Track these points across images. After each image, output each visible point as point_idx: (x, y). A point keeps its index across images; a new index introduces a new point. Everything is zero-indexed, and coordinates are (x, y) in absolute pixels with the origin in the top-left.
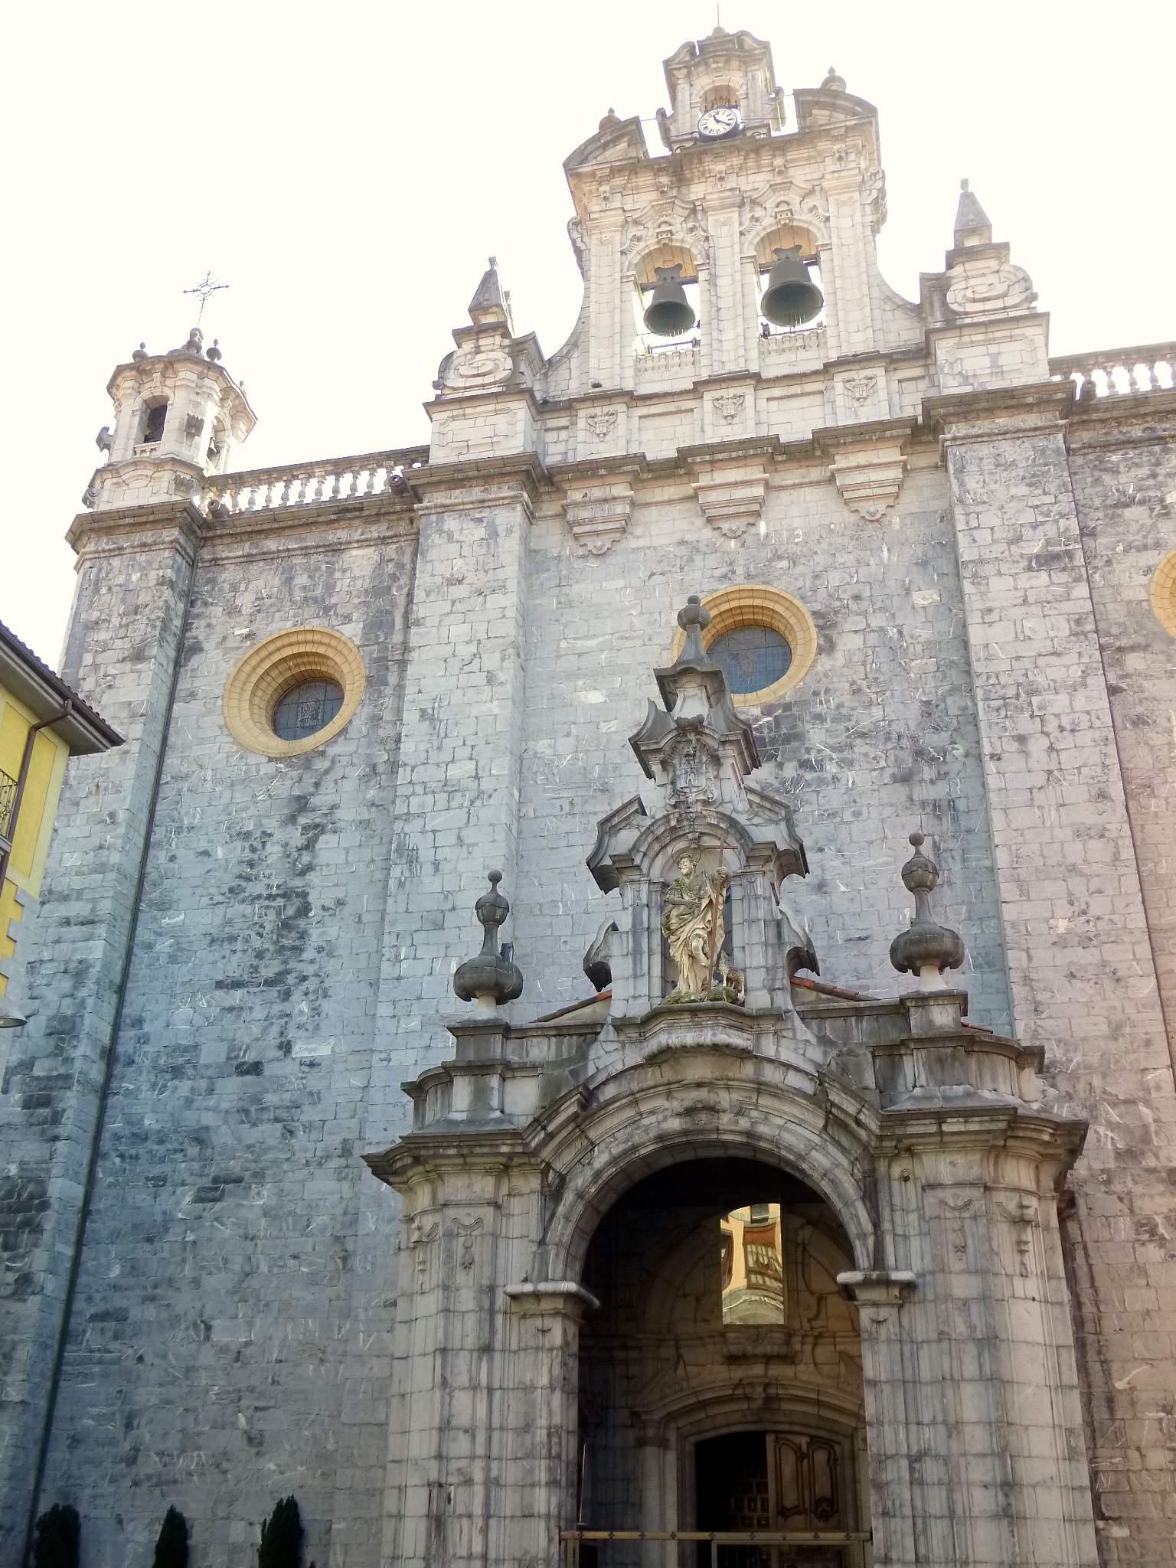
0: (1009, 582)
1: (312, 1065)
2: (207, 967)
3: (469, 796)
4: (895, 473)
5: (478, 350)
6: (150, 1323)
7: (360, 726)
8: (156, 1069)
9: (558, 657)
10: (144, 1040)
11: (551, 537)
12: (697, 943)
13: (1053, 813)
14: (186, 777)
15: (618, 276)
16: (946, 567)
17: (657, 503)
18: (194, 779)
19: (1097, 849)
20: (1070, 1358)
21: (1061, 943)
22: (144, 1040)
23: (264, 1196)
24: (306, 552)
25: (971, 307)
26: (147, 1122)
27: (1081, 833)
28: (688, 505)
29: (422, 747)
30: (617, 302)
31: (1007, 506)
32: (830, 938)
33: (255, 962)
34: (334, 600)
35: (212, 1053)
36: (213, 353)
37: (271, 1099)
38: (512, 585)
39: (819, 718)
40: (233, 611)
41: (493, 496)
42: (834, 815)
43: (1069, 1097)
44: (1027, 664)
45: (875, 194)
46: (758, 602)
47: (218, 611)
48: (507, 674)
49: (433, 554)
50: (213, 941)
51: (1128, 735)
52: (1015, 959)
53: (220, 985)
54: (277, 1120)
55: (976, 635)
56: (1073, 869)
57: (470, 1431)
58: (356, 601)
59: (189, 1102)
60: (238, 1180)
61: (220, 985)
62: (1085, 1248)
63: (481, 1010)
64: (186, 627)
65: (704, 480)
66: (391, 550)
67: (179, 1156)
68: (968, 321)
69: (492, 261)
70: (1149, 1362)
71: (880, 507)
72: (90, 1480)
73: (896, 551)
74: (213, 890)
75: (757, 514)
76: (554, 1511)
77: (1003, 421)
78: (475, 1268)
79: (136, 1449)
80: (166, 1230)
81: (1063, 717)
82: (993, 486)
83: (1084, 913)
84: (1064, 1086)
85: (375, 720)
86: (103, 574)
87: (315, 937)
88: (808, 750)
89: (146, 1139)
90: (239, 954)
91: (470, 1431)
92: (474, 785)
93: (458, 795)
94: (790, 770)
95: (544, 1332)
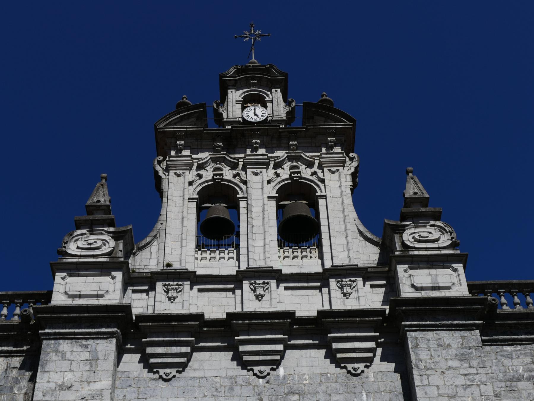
25: (417, 245)
31: (447, 372)
49: (50, 366)
71: (361, 366)
73: (372, 396)
82: (437, 359)
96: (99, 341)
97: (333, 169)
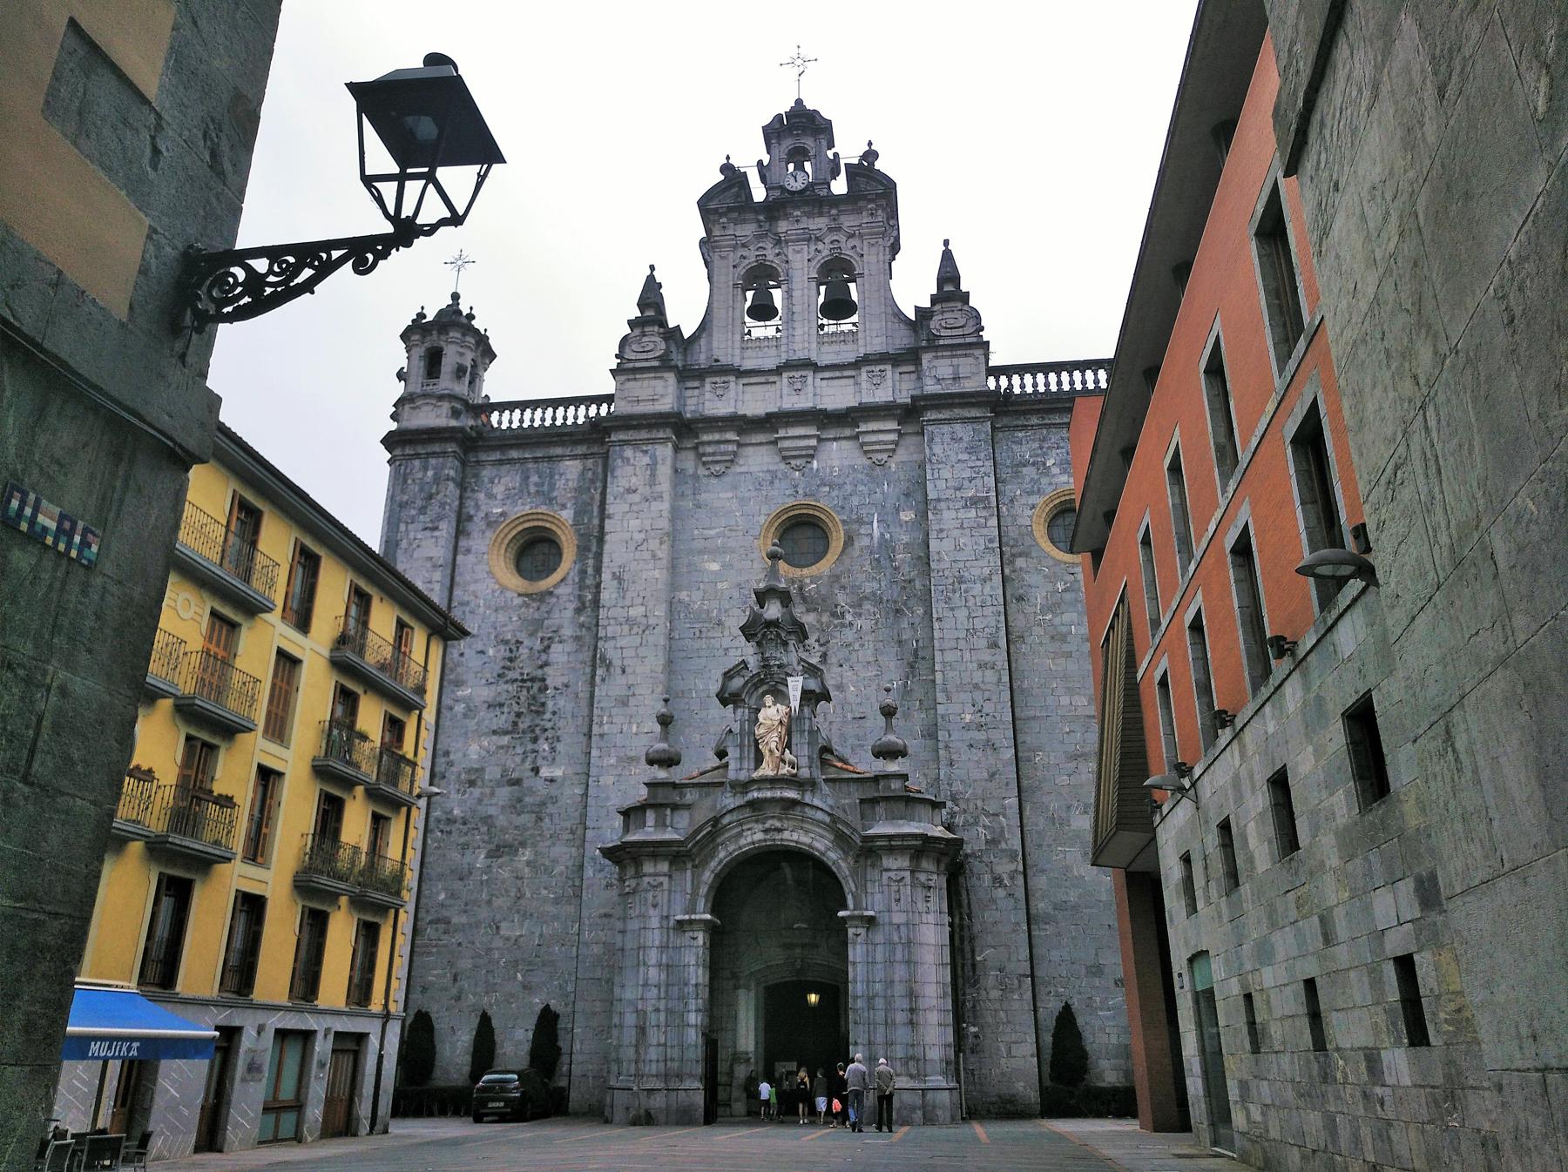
0: (952, 514)
1: (552, 781)
2: (486, 722)
3: (642, 628)
4: (893, 437)
5: (644, 334)
6: (463, 925)
7: (574, 576)
8: (461, 783)
9: (693, 539)
10: (451, 764)
11: (688, 462)
12: (773, 745)
13: (968, 653)
14: (467, 603)
15: (731, 283)
16: (920, 498)
17: (752, 444)
18: (472, 605)
19: (990, 675)
20: (947, 950)
21: (967, 728)
22: (451, 764)
23: (526, 855)
24: (536, 460)
26: (455, 812)
27: (982, 666)
28: (771, 447)
29: (614, 596)
30: (731, 302)
32: (844, 717)
33: (516, 719)
34: (555, 494)
35: (493, 773)
36: (471, 317)
37: (527, 799)
38: (666, 496)
39: (844, 588)
40: (490, 496)
41: (653, 436)
42: (850, 645)
43: (965, 811)
44: (961, 565)
45: (892, 240)
46: (811, 512)
47: (482, 496)
48: (663, 553)
49: (618, 472)
50: (489, 707)
51: (1013, 607)
52: (942, 735)
53: (495, 732)
54: (532, 812)
55: (933, 544)
56: (976, 686)
57: (658, 986)
58: (569, 495)
59: (480, 801)
60: (511, 846)
61: (495, 732)
62: (967, 890)
63: (661, 774)
64: (461, 505)
65: (782, 433)
66: (590, 462)
67: (476, 832)
68: (941, 342)
69: (652, 268)
70: (993, 947)
71: (884, 456)
72: (435, 1009)
74: (489, 675)
75: (812, 456)
76: (699, 1023)
77: (958, 412)
78: (659, 907)
79: (461, 991)
80: (471, 873)
81: (977, 598)
82: (949, 453)
83: (980, 711)
84: (963, 806)
85: (583, 573)
86: (408, 471)
87: (550, 704)
88: (836, 606)
89: (455, 822)
90: (505, 715)
91: (658, 986)
92: (644, 621)
93: (635, 627)
94: (825, 618)
95: (694, 939)
96: (656, 446)
97: (873, 241)
